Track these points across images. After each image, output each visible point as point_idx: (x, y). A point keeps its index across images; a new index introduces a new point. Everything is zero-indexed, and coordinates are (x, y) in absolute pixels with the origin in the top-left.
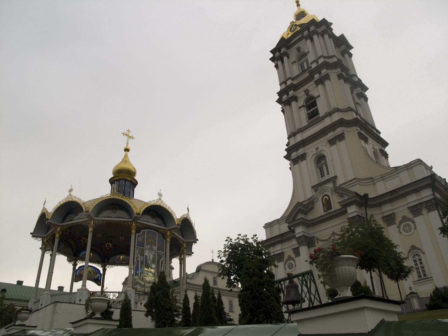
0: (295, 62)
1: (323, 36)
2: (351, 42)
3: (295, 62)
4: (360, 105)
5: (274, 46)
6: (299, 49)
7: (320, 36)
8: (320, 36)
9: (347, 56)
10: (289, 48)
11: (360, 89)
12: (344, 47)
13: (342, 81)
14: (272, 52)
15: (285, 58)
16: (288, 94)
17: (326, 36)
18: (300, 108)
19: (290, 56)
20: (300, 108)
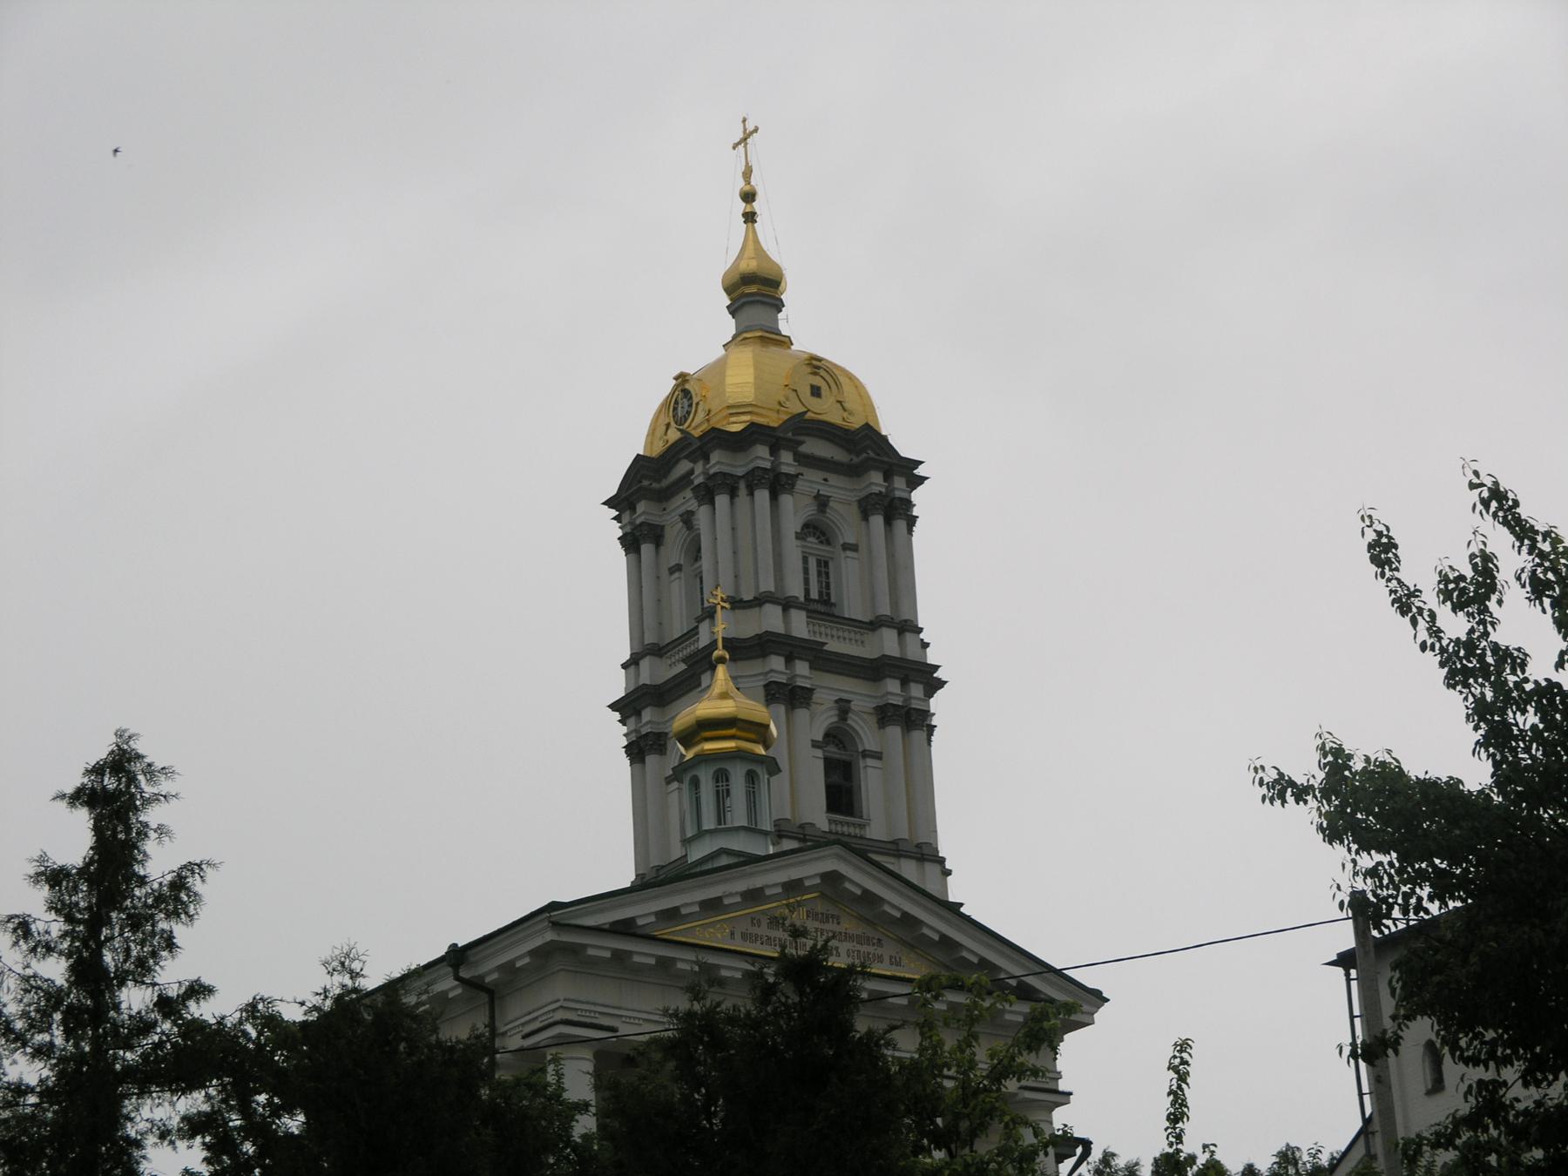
0: (677, 568)
1: (751, 494)
2: (905, 449)
3: (677, 568)
4: (878, 756)
5: (612, 491)
6: (688, 519)
7: (743, 491)
8: (743, 491)
9: (877, 521)
10: (663, 496)
11: (893, 686)
12: (876, 481)
13: (781, 709)
14: (609, 503)
15: (647, 549)
16: (638, 714)
17: (762, 496)
18: (669, 780)
19: (668, 531)
20: (669, 780)
